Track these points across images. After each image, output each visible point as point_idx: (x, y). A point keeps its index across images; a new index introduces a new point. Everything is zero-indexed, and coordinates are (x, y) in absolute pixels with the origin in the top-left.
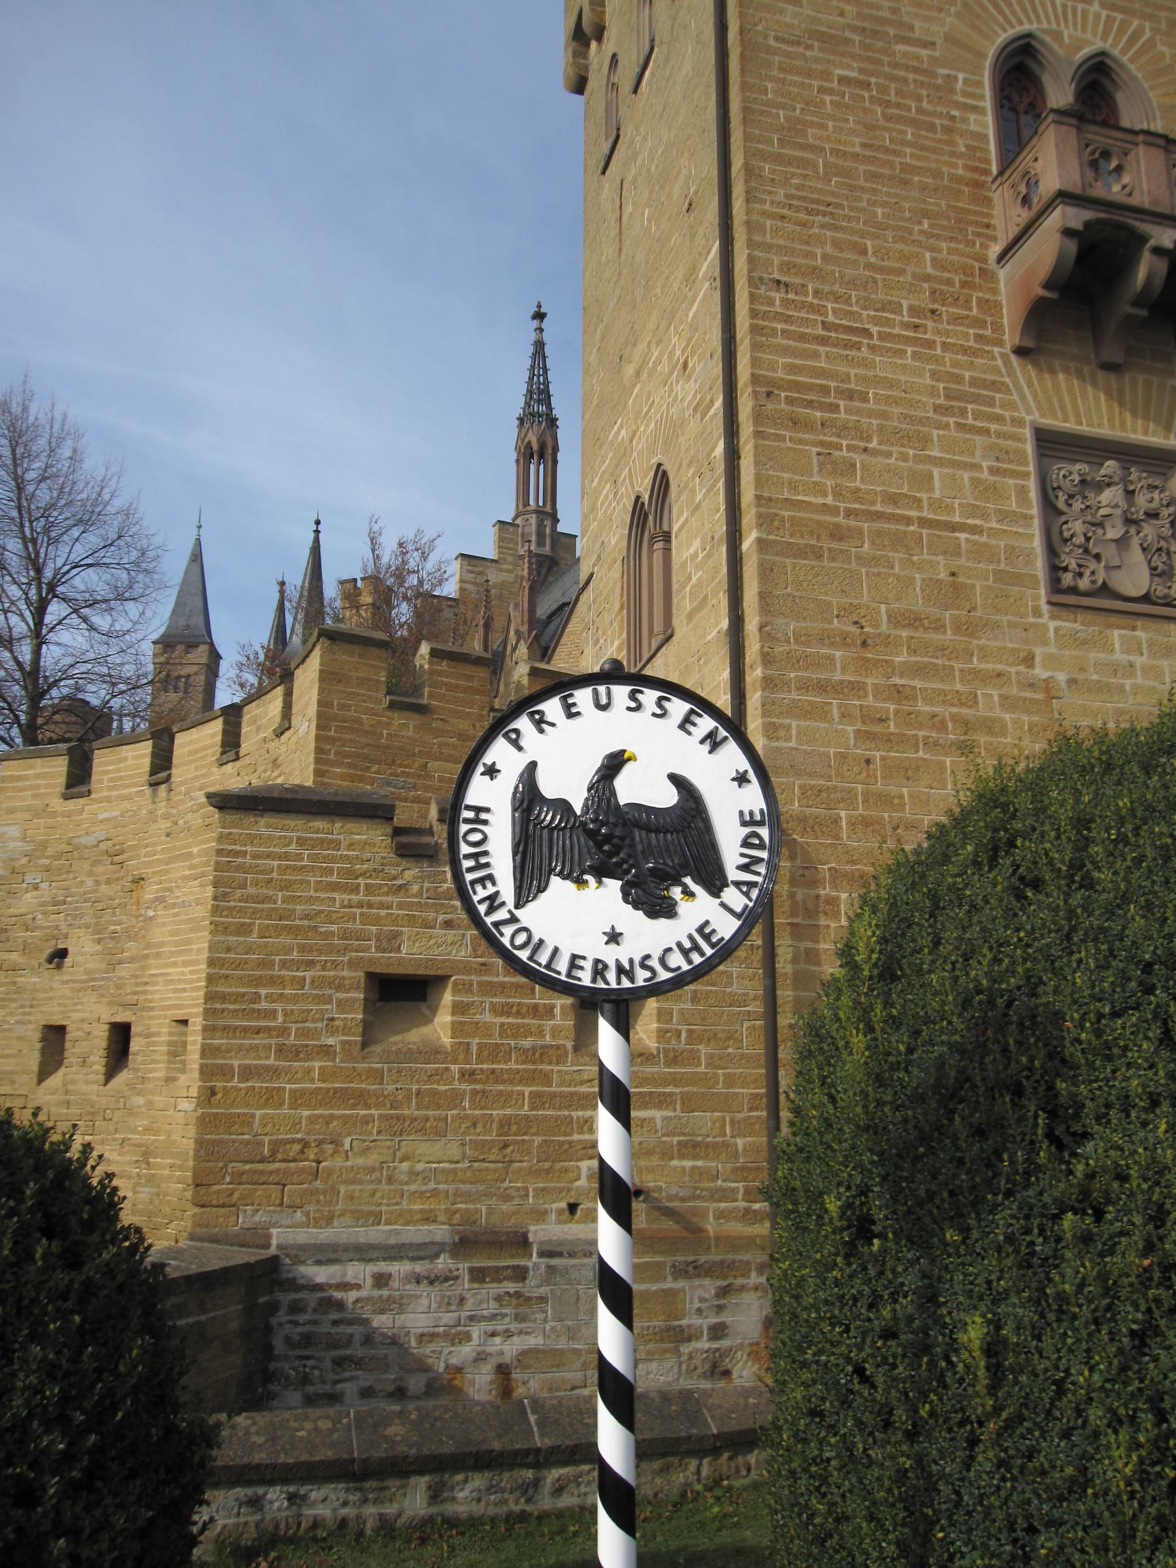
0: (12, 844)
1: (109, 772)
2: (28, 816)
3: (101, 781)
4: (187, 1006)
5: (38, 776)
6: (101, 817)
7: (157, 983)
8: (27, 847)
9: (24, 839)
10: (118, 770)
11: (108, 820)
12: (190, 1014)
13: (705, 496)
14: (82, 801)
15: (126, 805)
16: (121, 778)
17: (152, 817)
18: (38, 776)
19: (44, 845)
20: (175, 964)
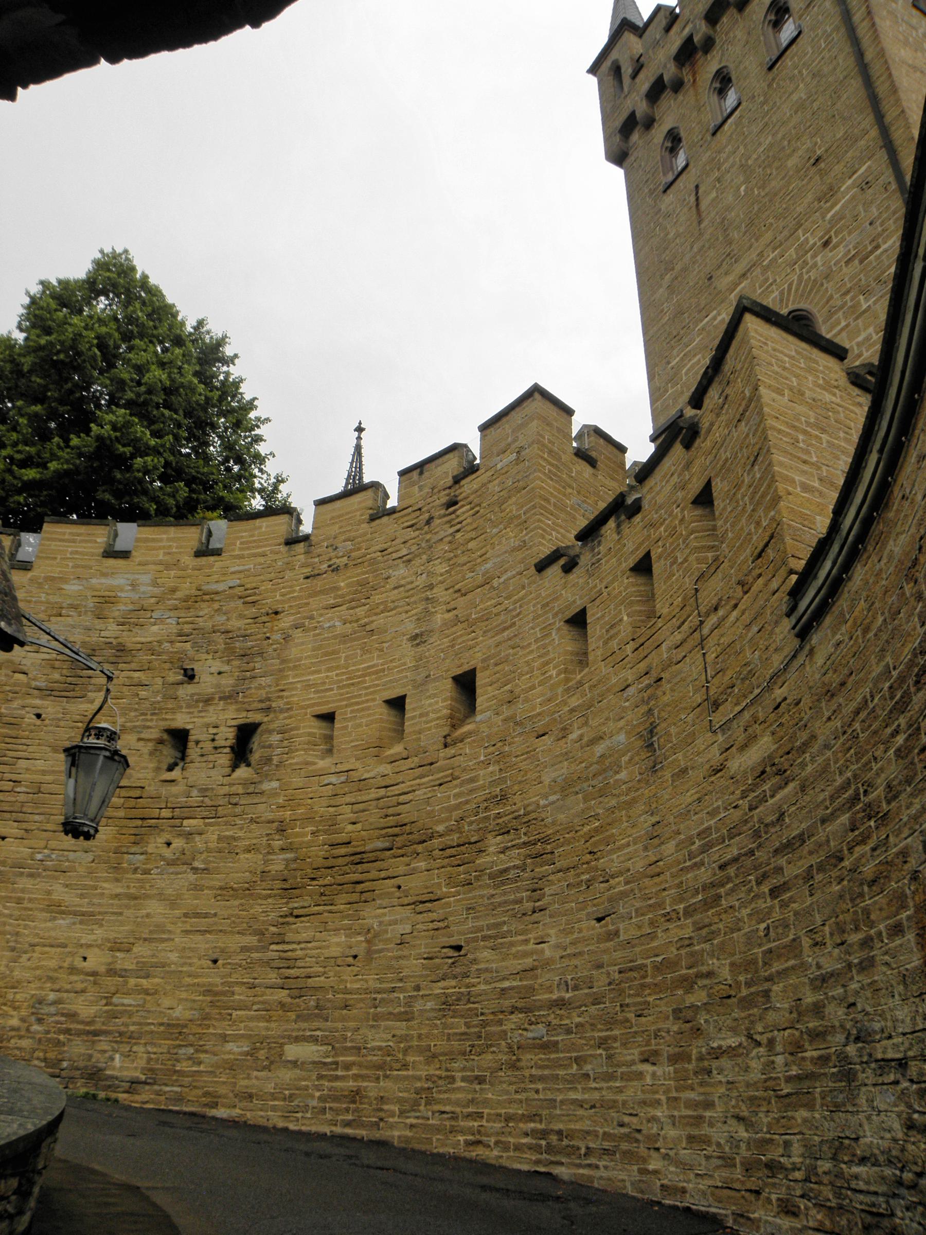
0: (143, 589)
1: (242, 537)
2: (160, 568)
3: (235, 544)
4: (334, 701)
5: (169, 540)
6: (232, 569)
7: (296, 689)
8: (156, 591)
9: (155, 584)
10: (253, 536)
11: (240, 572)
12: (340, 707)
13: (875, 303)
14: (212, 559)
15: (262, 560)
16: (254, 541)
17: (289, 566)
18: (169, 540)
19: (174, 590)
20: (319, 672)
